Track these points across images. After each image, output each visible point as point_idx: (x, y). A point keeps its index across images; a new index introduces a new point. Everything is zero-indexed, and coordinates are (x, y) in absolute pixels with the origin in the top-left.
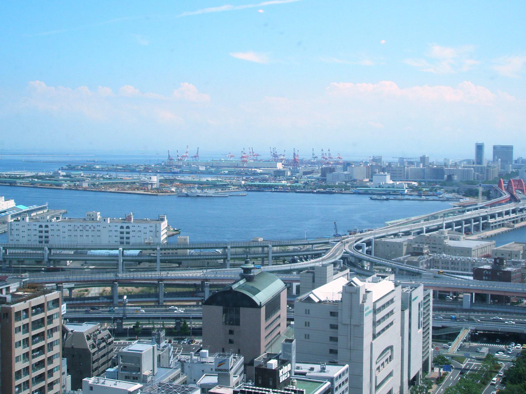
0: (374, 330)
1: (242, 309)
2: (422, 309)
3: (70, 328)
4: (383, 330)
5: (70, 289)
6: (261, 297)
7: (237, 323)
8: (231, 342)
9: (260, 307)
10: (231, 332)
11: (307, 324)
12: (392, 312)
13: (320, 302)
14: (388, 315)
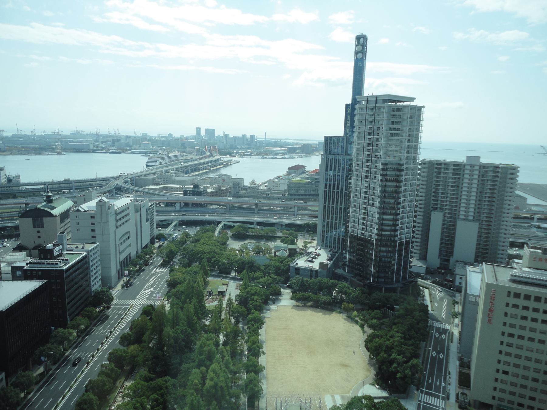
0: (116, 224)
2: (148, 212)
4: (123, 223)
8: (39, 237)
9: (56, 216)
10: (39, 232)
11: (78, 224)
12: (128, 214)
13: (85, 211)
14: (126, 216)
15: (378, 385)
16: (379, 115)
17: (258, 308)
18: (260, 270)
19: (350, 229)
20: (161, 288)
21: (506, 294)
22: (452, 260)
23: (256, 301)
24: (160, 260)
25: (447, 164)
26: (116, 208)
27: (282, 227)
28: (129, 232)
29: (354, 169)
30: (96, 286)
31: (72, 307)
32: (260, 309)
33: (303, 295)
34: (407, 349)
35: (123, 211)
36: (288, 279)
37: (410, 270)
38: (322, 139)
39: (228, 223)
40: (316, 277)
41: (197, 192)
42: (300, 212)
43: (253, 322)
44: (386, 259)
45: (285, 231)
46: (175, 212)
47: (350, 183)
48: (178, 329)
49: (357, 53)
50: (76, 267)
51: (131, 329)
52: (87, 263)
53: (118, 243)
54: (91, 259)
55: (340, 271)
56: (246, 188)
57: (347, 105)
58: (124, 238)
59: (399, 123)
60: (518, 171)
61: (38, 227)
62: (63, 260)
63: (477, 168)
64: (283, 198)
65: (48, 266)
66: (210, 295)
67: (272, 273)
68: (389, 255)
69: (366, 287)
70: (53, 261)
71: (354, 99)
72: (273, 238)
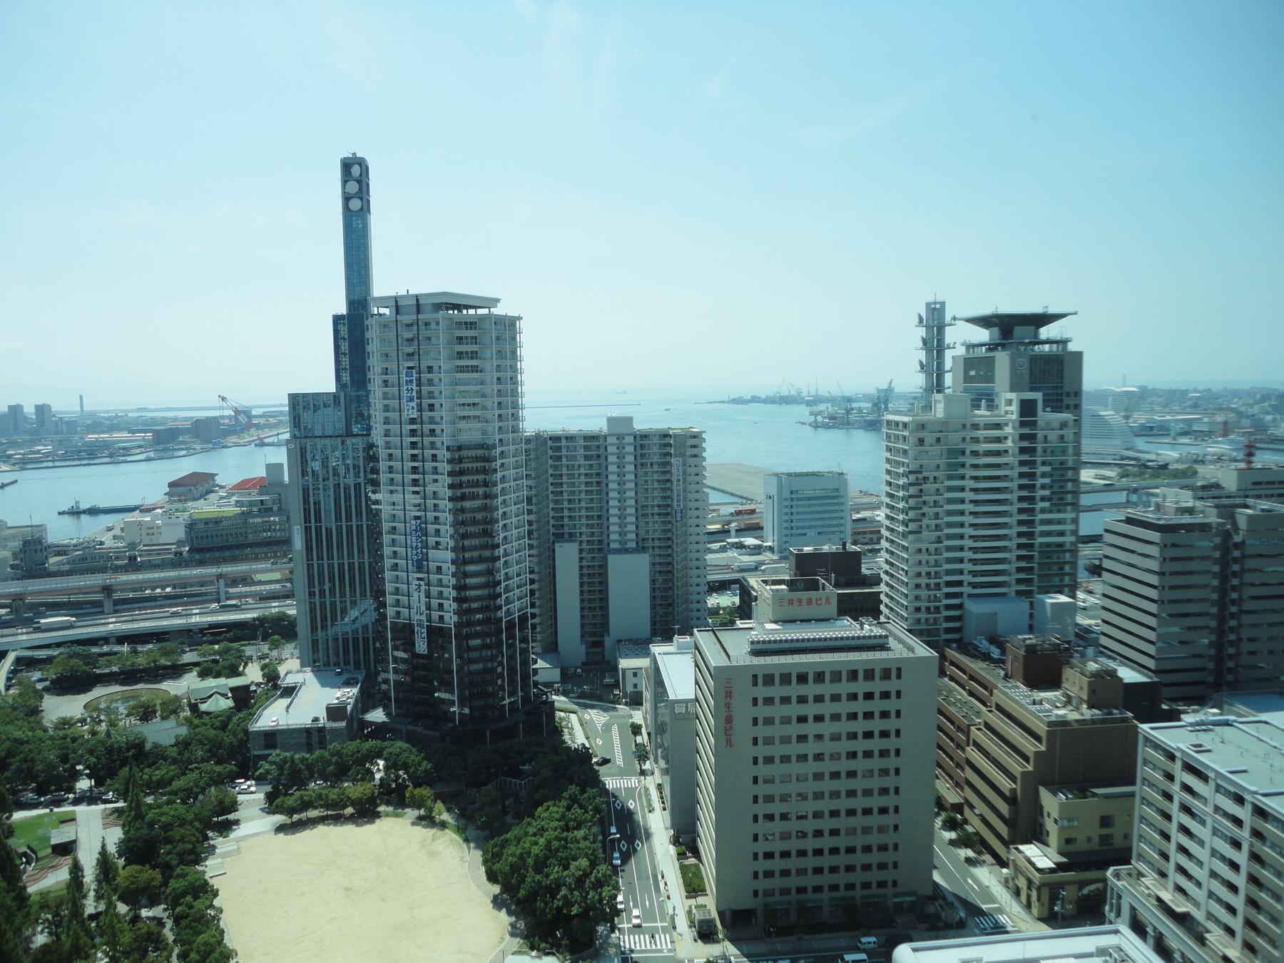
18: (165, 759)
19: (390, 612)
21: (751, 679)
22: (608, 642)
25: (571, 438)
27: (191, 637)
33: (301, 797)
37: (535, 678)
38: (283, 405)
40: (323, 744)
42: (232, 590)
49: (347, 198)
56: (61, 551)
57: (337, 320)
59: (473, 355)
60: (704, 440)
63: (631, 439)
64: (179, 561)
67: (203, 760)
69: (448, 739)
71: (351, 303)
72: (177, 671)
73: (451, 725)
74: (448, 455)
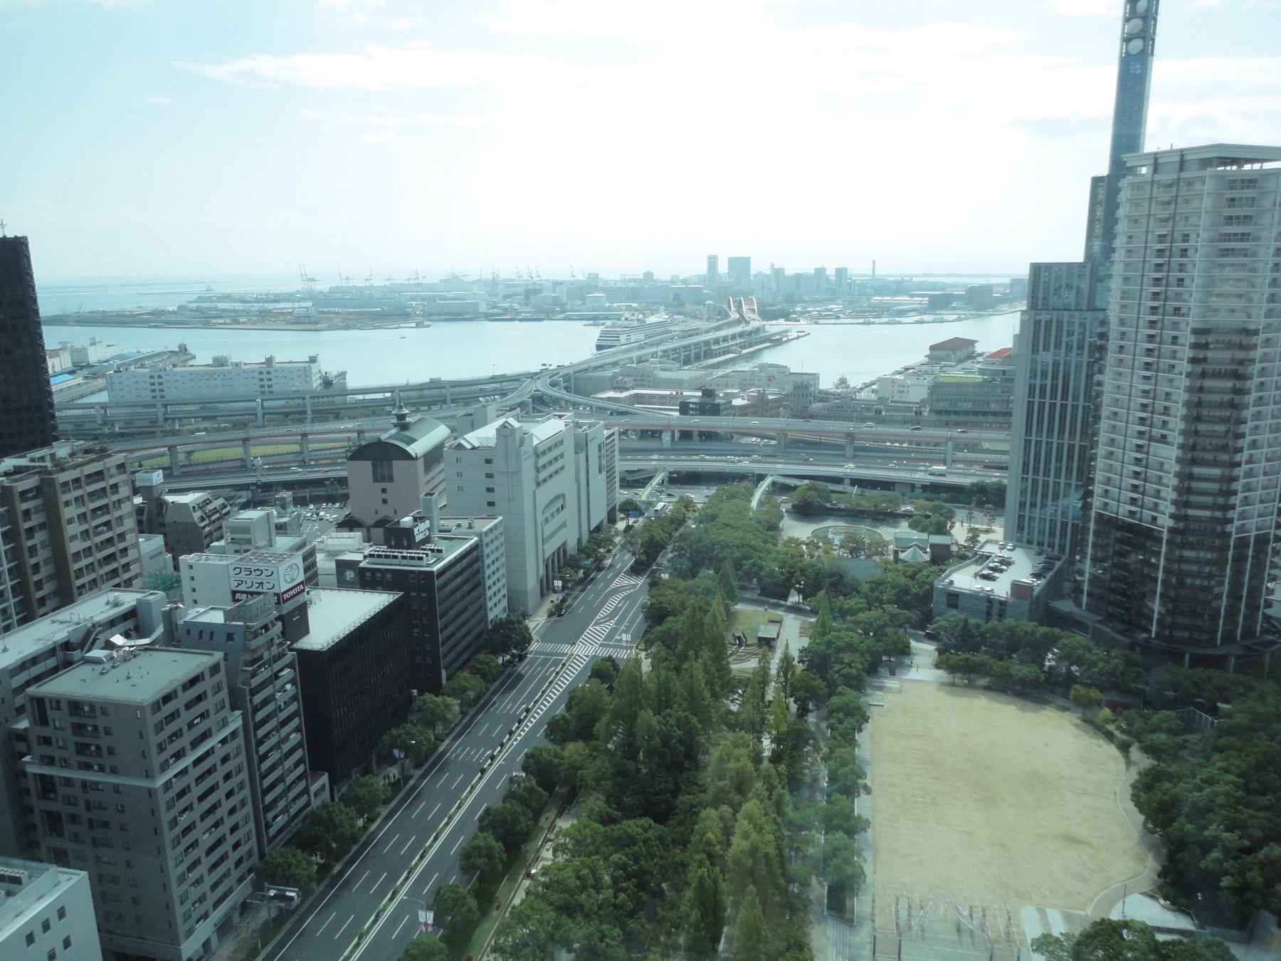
0: (537, 477)
1: (394, 462)
3: (170, 498)
4: (551, 476)
5: (190, 453)
6: (418, 448)
7: (390, 479)
8: (385, 501)
9: (416, 459)
12: (562, 455)
13: (474, 448)
14: (556, 459)
15: (1166, 898)
16: (1187, 202)
17: (855, 682)
18: (858, 593)
19: (1097, 502)
20: (632, 622)
23: (850, 665)
24: (629, 560)
26: (536, 442)
27: (913, 491)
28: (563, 495)
29: (1112, 345)
30: (496, 610)
31: (449, 652)
32: (857, 684)
33: (967, 660)
34: (1252, 817)
35: (550, 449)
36: (927, 618)
38: (1024, 272)
39: (782, 480)
40: (1002, 615)
41: (709, 406)
42: (959, 455)
43: (841, 715)
44: (1198, 582)
45: (922, 502)
46: (661, 451)
47: (1100, 384)
48: (670, 716)
49: (1127, 40)
50: (458, 567)
51: (569, 708)
52: (478, 559)
53: (540, 518)
54: (487, 551)
55: (1066, 606)
56: (824, 396)
57: (1096, 181)
58: (553, 509)
59: (1248, 219)
61: (383, 480)
62: (432, 551)
65: (404, 562)
66: (740, 645)
67: (890, 602)
68: (1207, 569)
70: (413, 553)
72: (890, 517)
73: (1144, 635)
74: (1192, 339)
